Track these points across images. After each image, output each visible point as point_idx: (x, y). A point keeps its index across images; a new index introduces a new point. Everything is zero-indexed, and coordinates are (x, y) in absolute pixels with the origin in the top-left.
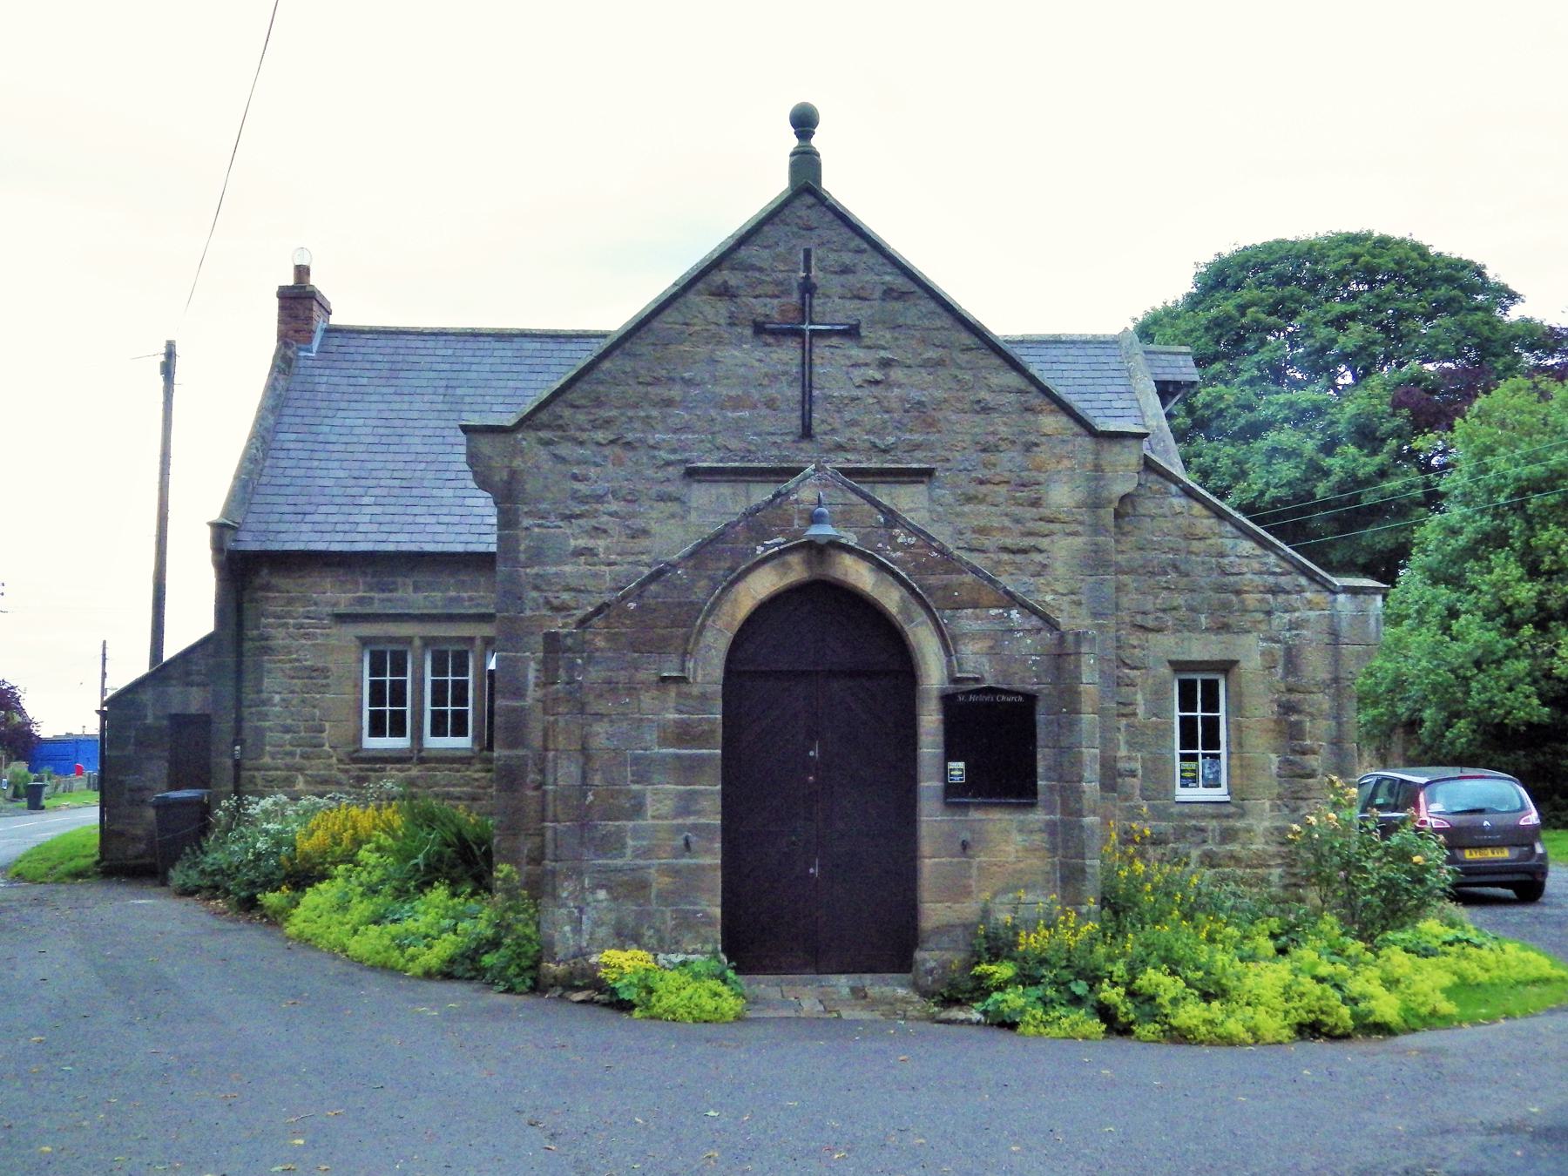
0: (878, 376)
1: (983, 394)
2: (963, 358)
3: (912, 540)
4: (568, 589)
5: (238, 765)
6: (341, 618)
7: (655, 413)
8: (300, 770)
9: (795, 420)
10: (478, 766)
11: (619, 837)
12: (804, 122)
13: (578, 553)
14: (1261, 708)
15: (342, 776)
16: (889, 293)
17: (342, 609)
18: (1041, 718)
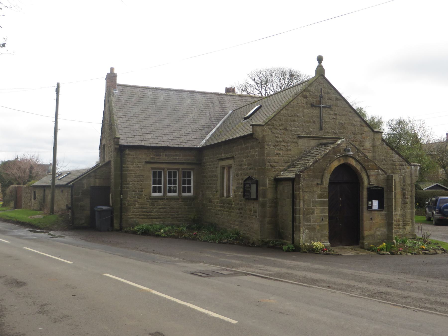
0: (334, 117)
1: (354, 122)
2: (350, 114)
3: (362, 155)
4: (275, 162)
5: (121, 200)
6: (147, 163)
8: (137, 201)
10: (181, 200)
12: (320, 59)
13: (277, 154)
15: (148, 203)
18: (385, 192)
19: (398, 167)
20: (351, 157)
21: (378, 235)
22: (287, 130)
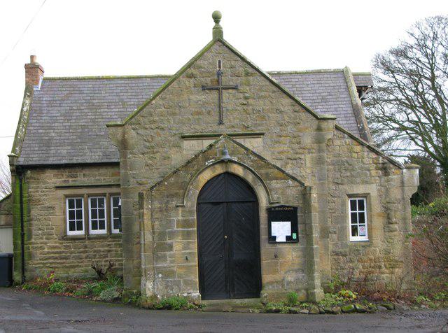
6: (58, 188)
10: (110, 239)
12: (216, 18)
14: (377, 208)
17: (58, 185)
20: (235, 162)
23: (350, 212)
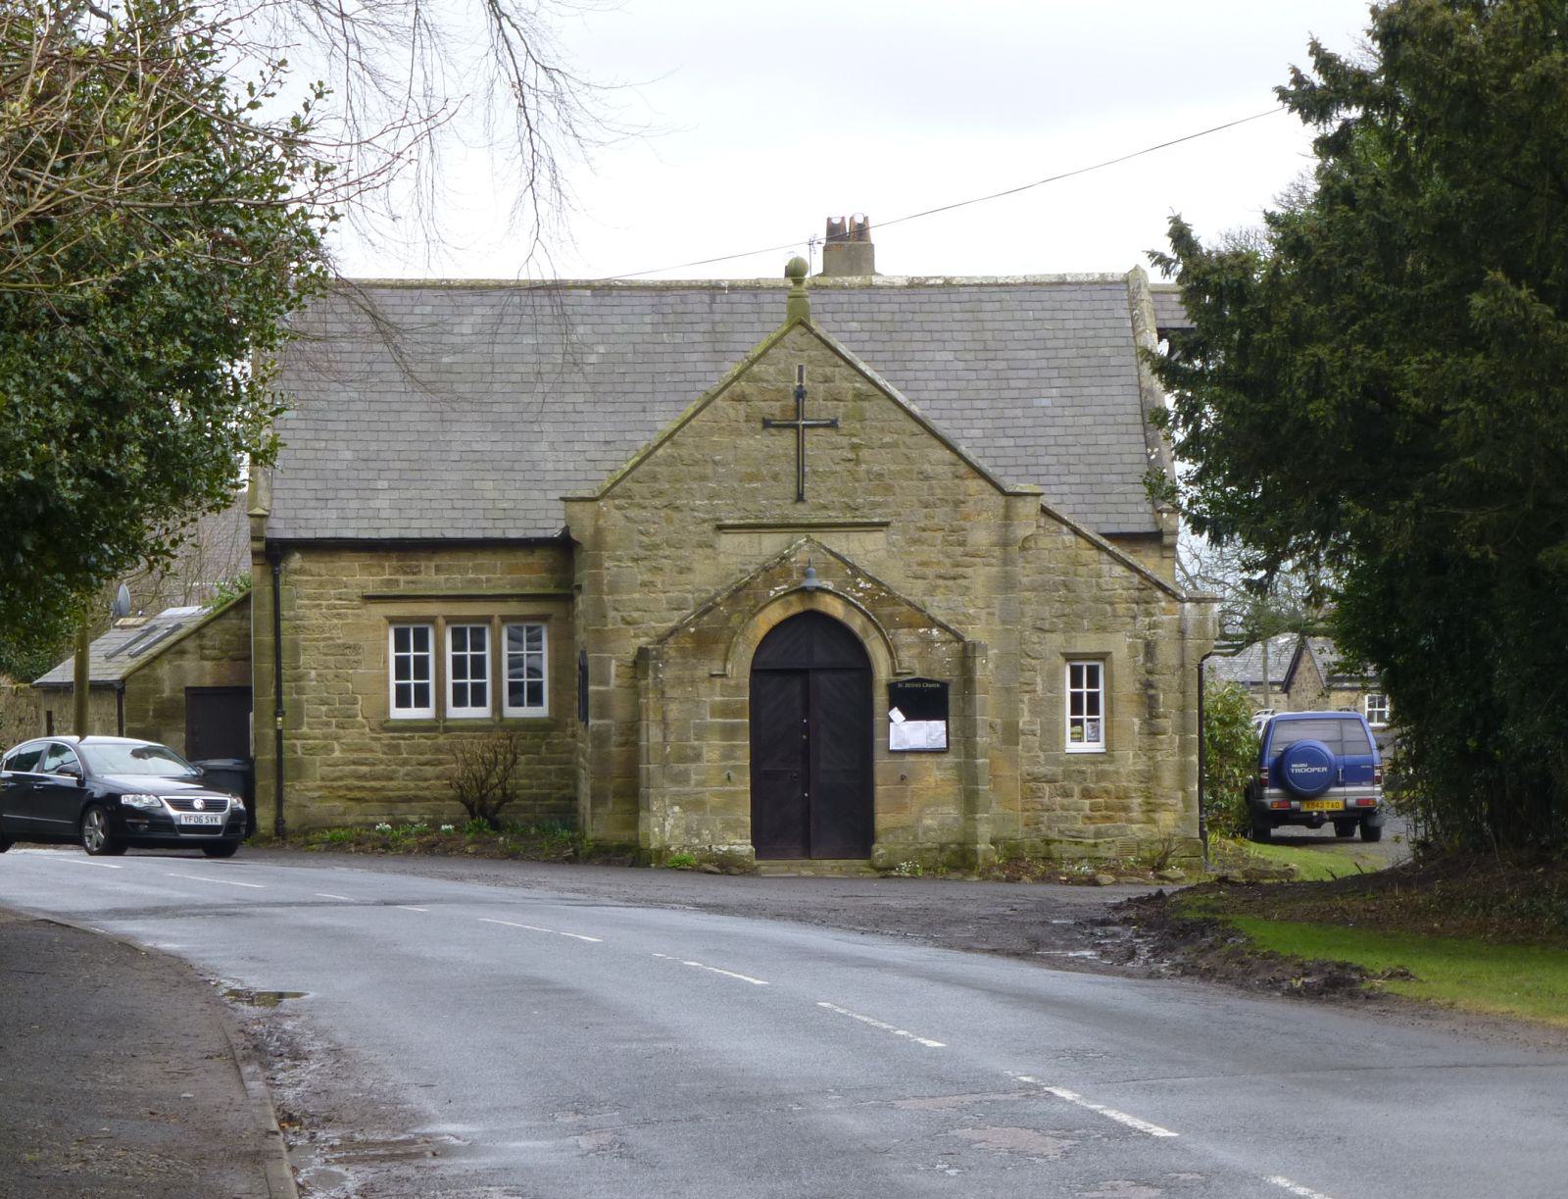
0: (850, 455)
1: (927, 467)
3: (869, 585)
4: (638, 610)
5: (279, 735)
6: (370, 599)
7: (695, 486)
8: (337, 738)
9: (793, 489)
11: (686, 772)
13: (644, 584)
14: (1128, 686)
15: (376, 745)
16: (859, 396)
17: (370, 591)
18: (951, 697)
19: (1121, 608)
21: (928, 829)
22: (677, 509)
23: (1068, 690)
